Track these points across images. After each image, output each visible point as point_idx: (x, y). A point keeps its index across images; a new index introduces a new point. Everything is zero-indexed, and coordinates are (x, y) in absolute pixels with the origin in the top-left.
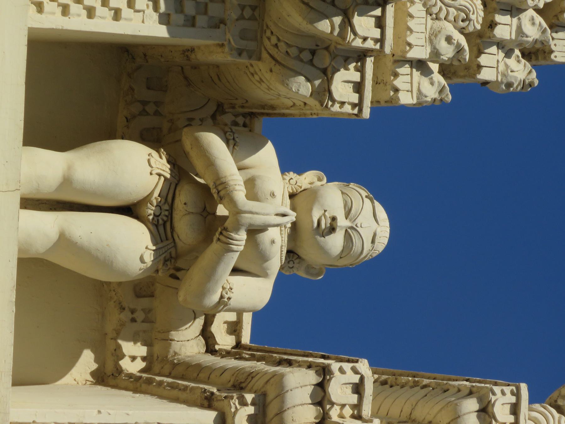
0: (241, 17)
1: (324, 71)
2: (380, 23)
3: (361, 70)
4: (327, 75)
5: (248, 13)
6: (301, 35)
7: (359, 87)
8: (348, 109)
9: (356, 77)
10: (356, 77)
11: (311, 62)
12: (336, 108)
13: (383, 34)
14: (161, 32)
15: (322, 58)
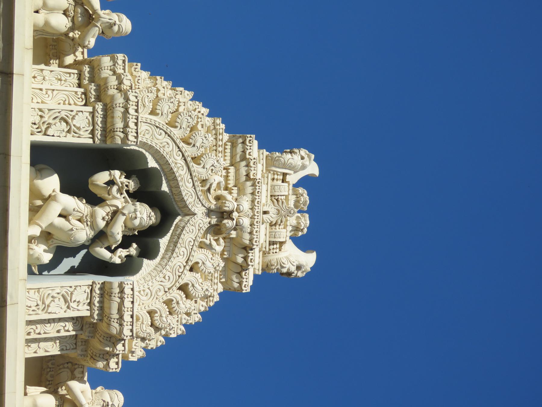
0: (82, 345)
1: (107, 360)
2: (124, 345)
3: (118, 358)
4: (108, 360)
5: (84, 343)
6: (101, 350)
7: (117, 363)
8: (114, 370)
9: (117, 360)
10: (116, 360)
11: (103, 358)
12: (111, 371)
13: (125, 348)
14: (59, 353)
15: (107, 356)
